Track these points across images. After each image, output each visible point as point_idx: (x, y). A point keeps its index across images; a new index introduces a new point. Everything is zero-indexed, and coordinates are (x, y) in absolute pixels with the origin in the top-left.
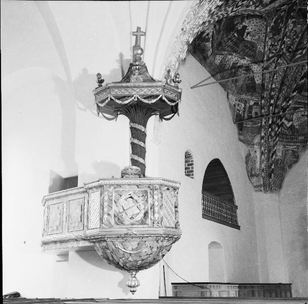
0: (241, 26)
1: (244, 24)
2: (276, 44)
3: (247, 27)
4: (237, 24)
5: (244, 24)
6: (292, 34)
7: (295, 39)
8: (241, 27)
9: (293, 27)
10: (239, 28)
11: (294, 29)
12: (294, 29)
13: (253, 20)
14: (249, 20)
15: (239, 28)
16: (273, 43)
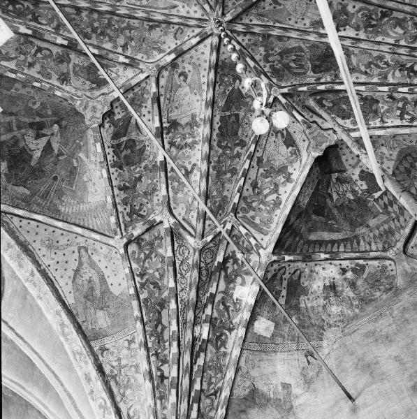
0: (359, 182)
1: (355, 177)
2: (400, 105)
3: (362, 171)
4: (354, 192)
5: (355, 177)
6: (376, 71)
7: (386, 63)
8: (363, 183)
9: (361, 72)
10: (365, 187)
11: (363, 68)
12: (363, 68)
13: (347, 160)
14: (348, 167)
15: (365, 187)
16: (398, 112)
